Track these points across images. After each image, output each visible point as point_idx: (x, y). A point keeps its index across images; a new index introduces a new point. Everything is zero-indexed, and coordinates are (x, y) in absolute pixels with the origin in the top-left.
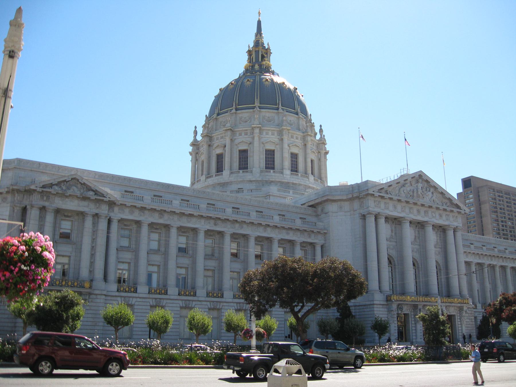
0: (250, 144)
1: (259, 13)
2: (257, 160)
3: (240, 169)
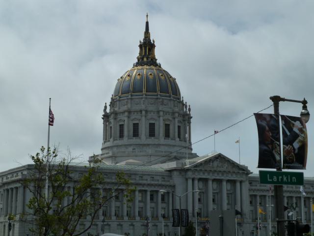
0: (140, 120)
1: (147, 16)
2: (144, 129)
3: (134, 136)
